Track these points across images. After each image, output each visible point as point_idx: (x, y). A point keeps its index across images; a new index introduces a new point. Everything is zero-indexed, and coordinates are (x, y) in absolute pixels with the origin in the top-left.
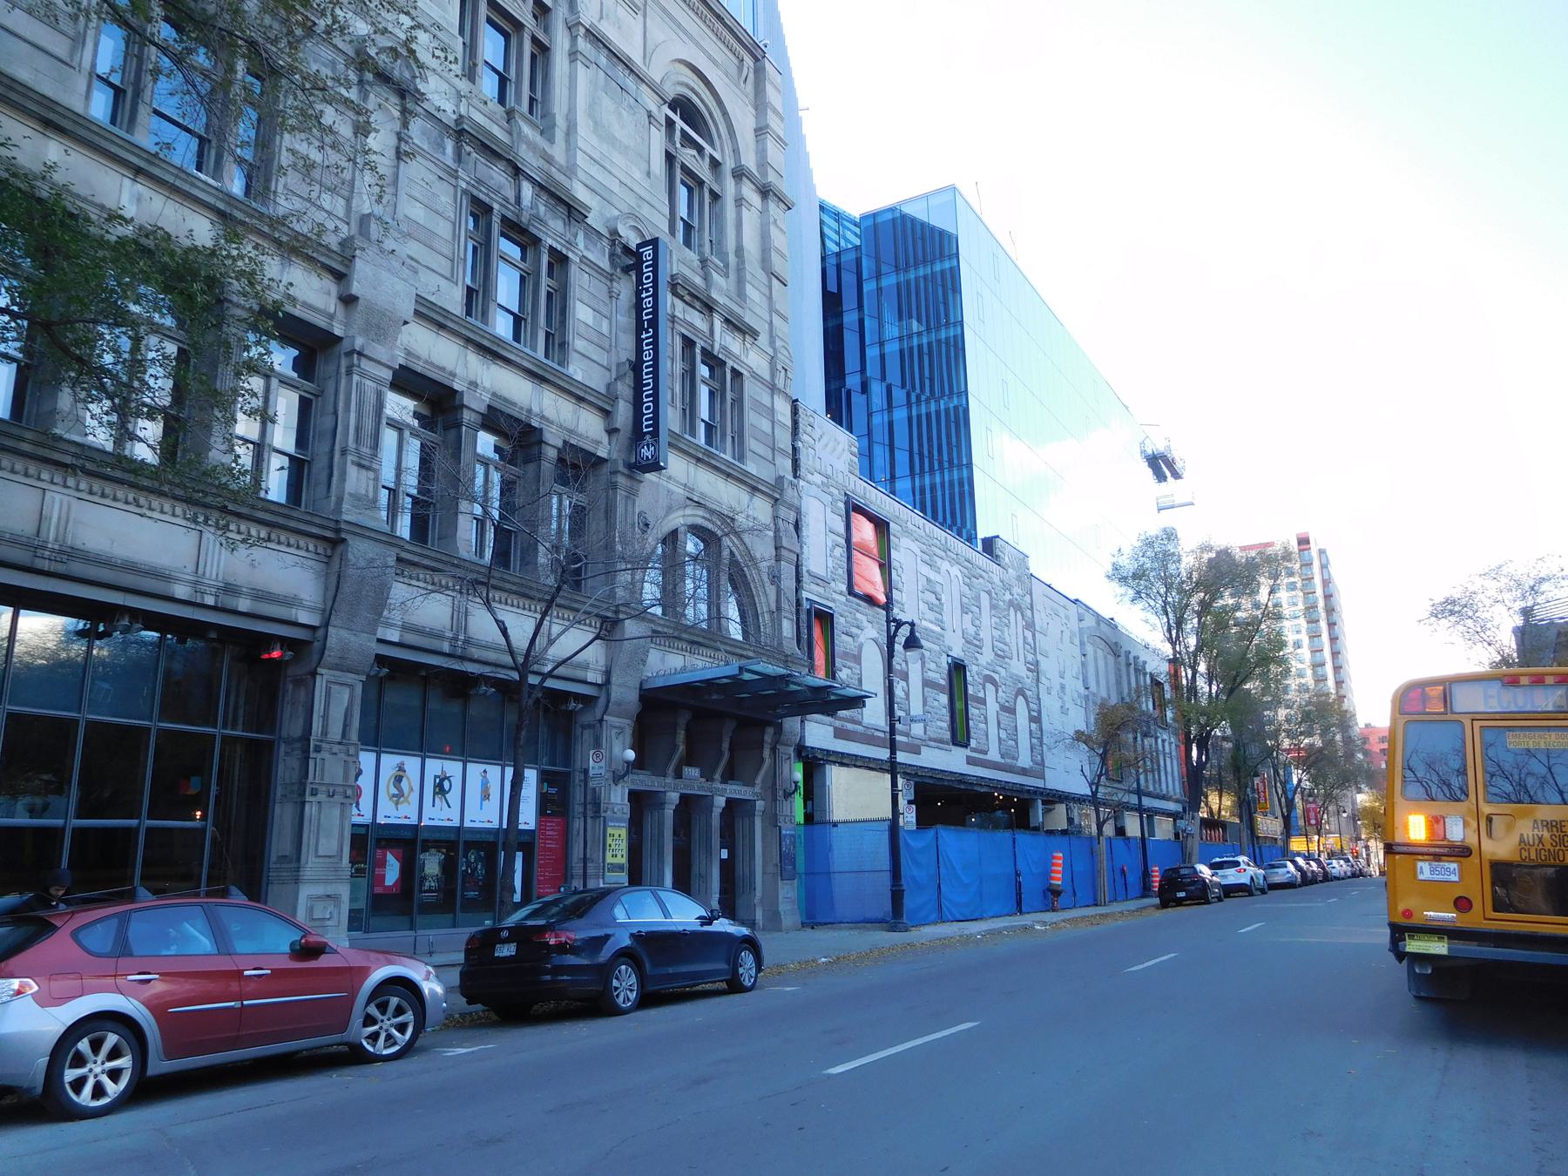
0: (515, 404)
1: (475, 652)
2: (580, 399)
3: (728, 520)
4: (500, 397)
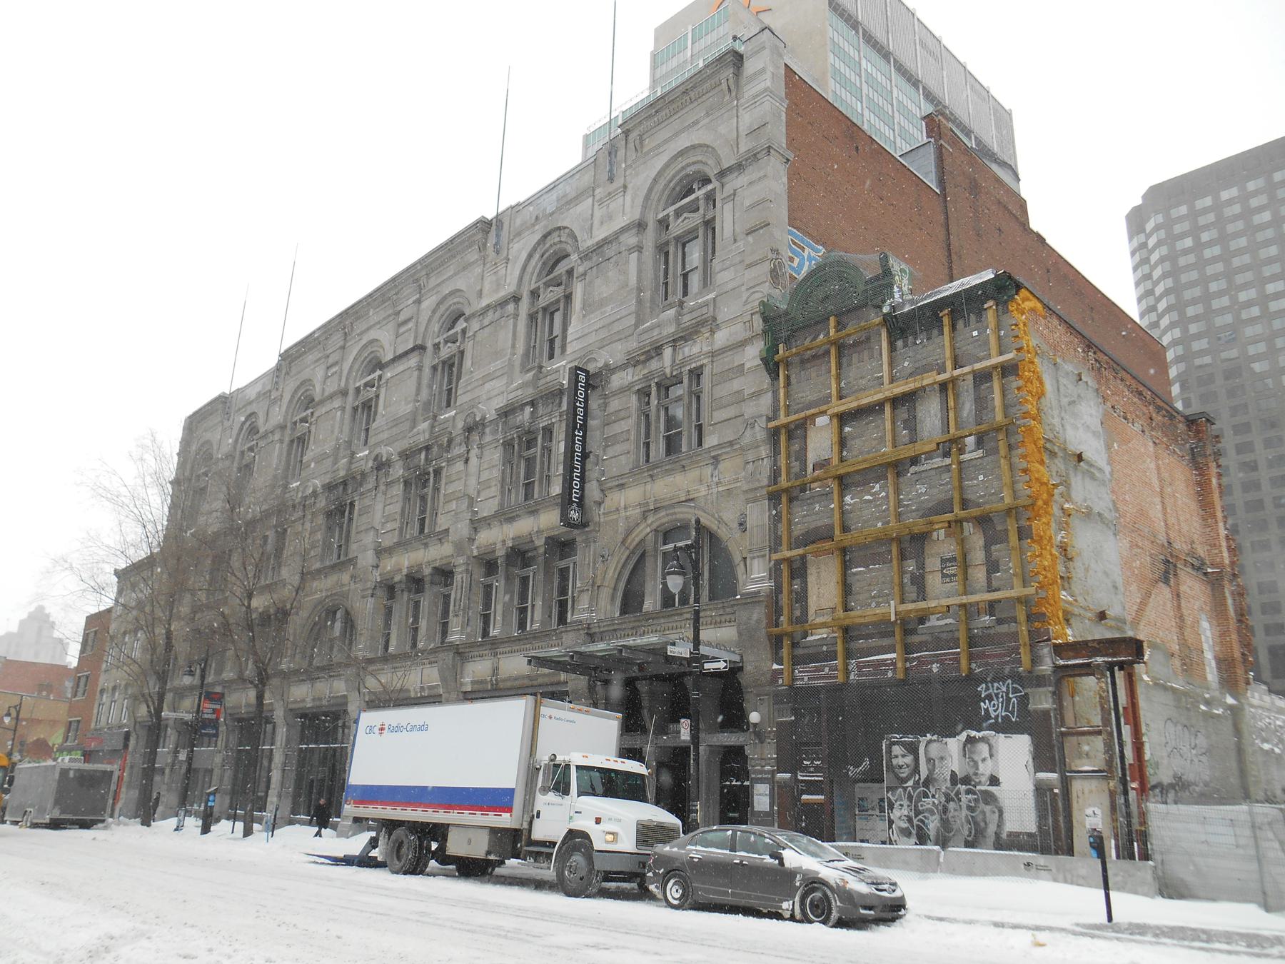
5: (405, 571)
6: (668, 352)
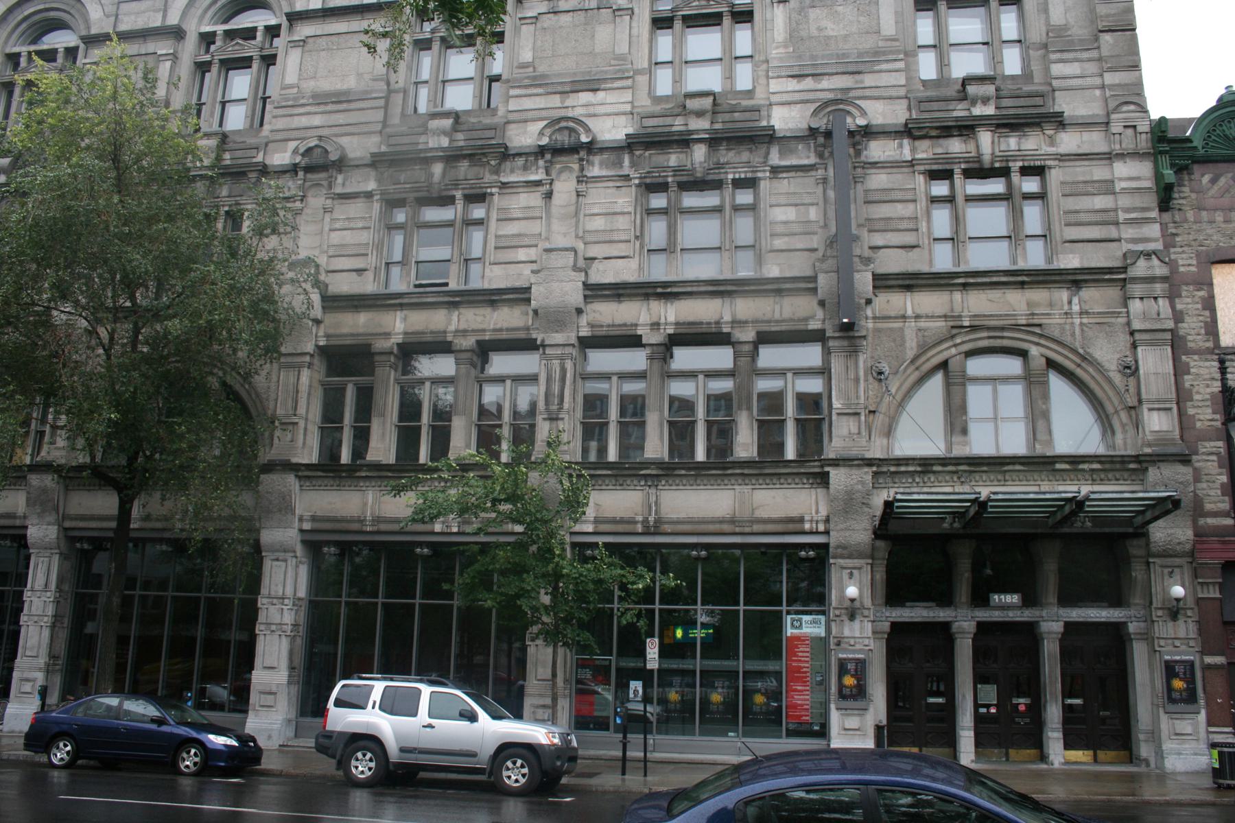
0: (701, 323)
1: (668, 528)
2: (779, 292)
3: (1033, 327)
4: (684, 323)
5: (399, 339)
6: (985, 138)
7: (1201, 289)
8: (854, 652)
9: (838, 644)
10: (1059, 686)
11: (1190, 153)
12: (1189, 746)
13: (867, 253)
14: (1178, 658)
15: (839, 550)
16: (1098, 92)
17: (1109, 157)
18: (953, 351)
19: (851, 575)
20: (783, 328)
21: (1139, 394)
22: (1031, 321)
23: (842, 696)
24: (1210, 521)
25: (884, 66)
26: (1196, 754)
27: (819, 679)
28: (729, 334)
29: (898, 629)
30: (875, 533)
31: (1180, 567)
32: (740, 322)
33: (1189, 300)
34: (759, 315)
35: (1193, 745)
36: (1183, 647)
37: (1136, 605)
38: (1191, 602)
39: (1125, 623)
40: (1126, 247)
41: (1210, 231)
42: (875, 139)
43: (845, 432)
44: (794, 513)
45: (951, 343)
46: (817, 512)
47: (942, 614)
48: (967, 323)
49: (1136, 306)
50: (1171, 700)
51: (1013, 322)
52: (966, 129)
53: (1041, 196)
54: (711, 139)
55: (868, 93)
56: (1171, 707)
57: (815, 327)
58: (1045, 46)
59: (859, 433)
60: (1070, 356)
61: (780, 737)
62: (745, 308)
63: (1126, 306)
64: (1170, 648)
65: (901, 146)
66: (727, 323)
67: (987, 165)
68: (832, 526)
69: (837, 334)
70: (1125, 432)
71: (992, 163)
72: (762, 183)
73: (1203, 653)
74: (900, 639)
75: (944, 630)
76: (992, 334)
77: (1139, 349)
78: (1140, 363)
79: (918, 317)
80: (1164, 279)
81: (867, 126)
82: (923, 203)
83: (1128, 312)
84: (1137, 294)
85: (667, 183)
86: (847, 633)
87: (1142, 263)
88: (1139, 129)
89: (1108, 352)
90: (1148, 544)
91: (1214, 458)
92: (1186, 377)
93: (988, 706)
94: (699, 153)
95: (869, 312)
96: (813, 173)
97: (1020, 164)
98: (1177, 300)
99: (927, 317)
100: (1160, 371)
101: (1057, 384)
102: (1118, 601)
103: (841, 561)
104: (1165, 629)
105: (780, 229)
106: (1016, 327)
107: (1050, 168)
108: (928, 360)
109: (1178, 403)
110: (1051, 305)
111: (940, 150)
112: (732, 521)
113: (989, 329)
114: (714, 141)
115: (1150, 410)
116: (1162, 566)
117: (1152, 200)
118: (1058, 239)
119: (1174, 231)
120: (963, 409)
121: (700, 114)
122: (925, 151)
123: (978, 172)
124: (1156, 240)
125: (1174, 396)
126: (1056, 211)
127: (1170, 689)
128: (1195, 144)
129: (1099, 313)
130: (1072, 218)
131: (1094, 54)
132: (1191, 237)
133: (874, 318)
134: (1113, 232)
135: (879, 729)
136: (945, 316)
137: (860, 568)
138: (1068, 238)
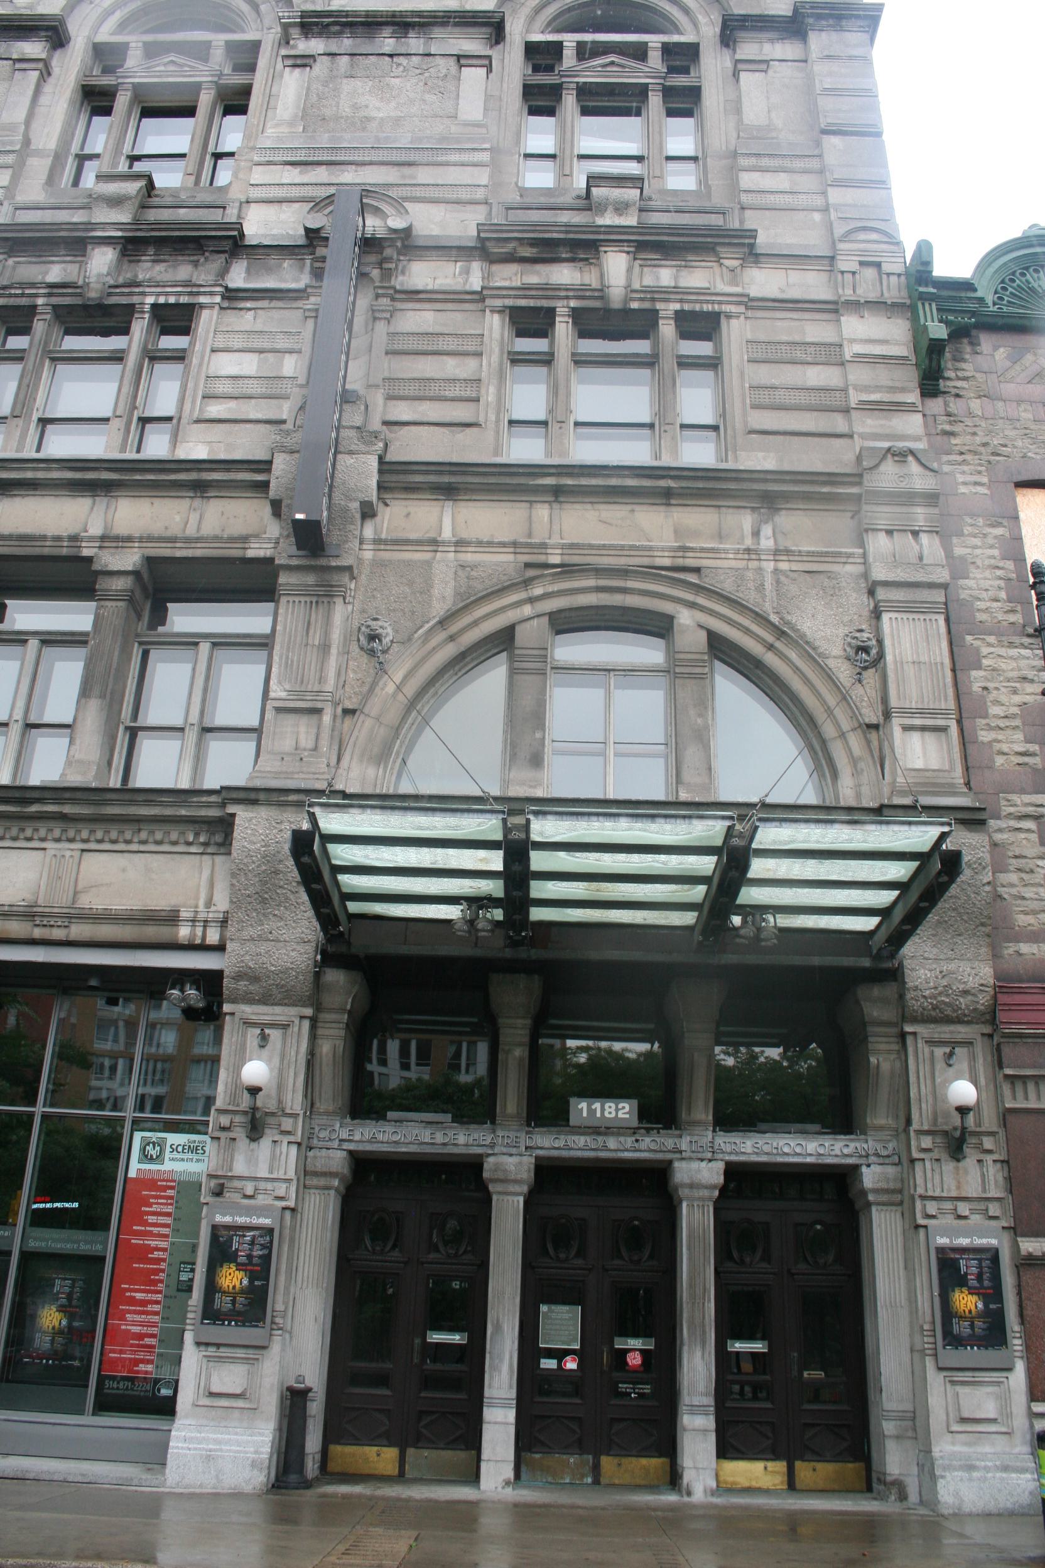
0: (44, 538)
2: (200, 488)
3: (682, 573)
7: (999, 525)
8: (249, 1211)
9: (219, 1193)
10: (711, 1306)
11: (972, 306)
12: (990, 1449)
13: (375, 425)
14: (964, 1242)
15: (243, 984)
16: (817, 216)
17: (833, 309)
18: (527, 610)
19: (264, 1039)
20: (199, 553)
21: (885, 700)
22: (680, 562)
23: (211, 1314)
24: (1025, 948)
25: (454, 157)
26: (1006, 1469)
27: (184, 1277)
28: (89, 560)
29: (366, 1169)
30: (324, 953)
31: (969, 1044)
32: (117, 539)
33: (977, 541)
34: (157, 529)
35: (1000, 1445)
36: (976, 1218)
37: (881, 1128)
38: (990, 1121)
39: (856, 1168)
40: (858, 443)
41: (1011, 433)
42: (420, 259)
43: (287, 745)
44: (159, 902)
45: (523, 595)
46: (209, 903)
47: (462, 1139)
48: (555, 560)
49: (879, 544)
50: (953, 1340)
51: (646, 561)
52: (583, 247)
53: (713, 364)
54: (128, 241)
55: (418, 192)
56: (952, 1356)
57: (261, 554)
58: (735, 155)
59: (315, 749)
60: (754, 628)
61: (80, 1412)
62: (133, 514)
63: (862, 544)
64: (949, 1220)
65: (467, 272)
66: (92, 539)
67: (616, 302)
68: (231, 930)
69: (295, 562)
70: (856, 773)
71: (627, 299)
72: (205, 314)
73: (1015, 1231)
74: (372, 1191)
75: (467, 1174)
76: (602, 582)
77: (885, 617)
78: (887, 642)
79: (460, 544)
80: (932, 499)
81: (407, 232)
82: (494, 356)
83: (864, 555)
84: (882, 523)
85: (35, 307)
86: (240, 1167)
87: (889, 467)
88: (886, 268)
89: (826, 624)
90: (901, 996)
91: (1030, 824)
92: (974, 673)
93: (560, 1355)
94: (101, 262)
95: (369, 532)
96: (299, 304)
97: (677, 306)
98: (955, 540)
99: (480, 543)
100: (924, 658)
101: (730, 691)
102: (843, 1119)
103: (247, 1010)
104: (937, 1177)
105: (222, 388)
106: (652, 572)
107: (729, 316)
108: (475, 623)
109: (959, 722)
110: (720, 537)
111: (533, 279)
112: (29, 914)
113: (599, 571)
114: (132, 246)
115: (907, 728)
116: (931, 1042)
117: (909, 377)
118: (739, 425)
119: (947, 427)
120: (538, 718)
121: (115, 202)
122: (509, 276)
123: (601, 320)
124: (917, 439)
125: (951, 704)
126: (736, 382)
127: (948, 1313)
128: (979, 294)
129: (809, 554)
130: (765, 398)
131: (814, 164)
132: (978, 440)
133: (377, 541)
134: (839, 423)
135: (295, 1399)
136: (515, 544)
137: (285, 1027)
138: (758, 427)
